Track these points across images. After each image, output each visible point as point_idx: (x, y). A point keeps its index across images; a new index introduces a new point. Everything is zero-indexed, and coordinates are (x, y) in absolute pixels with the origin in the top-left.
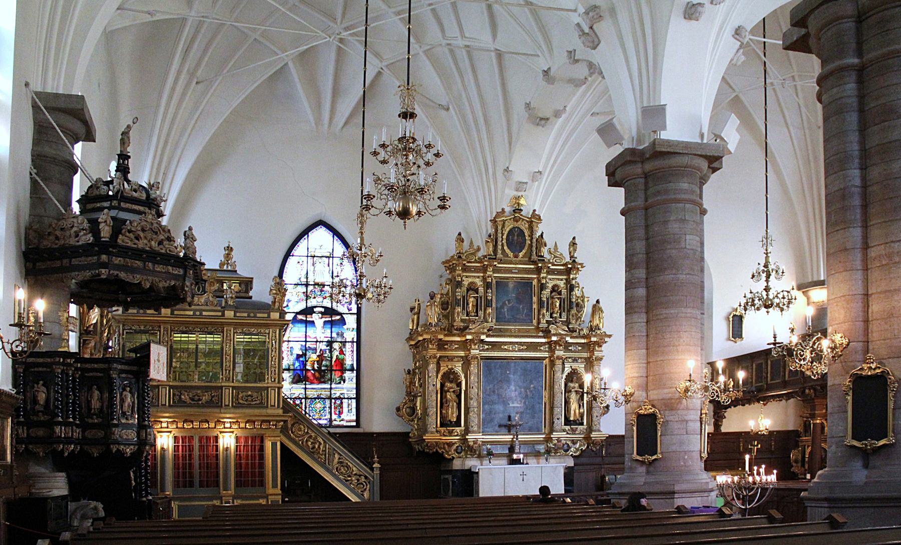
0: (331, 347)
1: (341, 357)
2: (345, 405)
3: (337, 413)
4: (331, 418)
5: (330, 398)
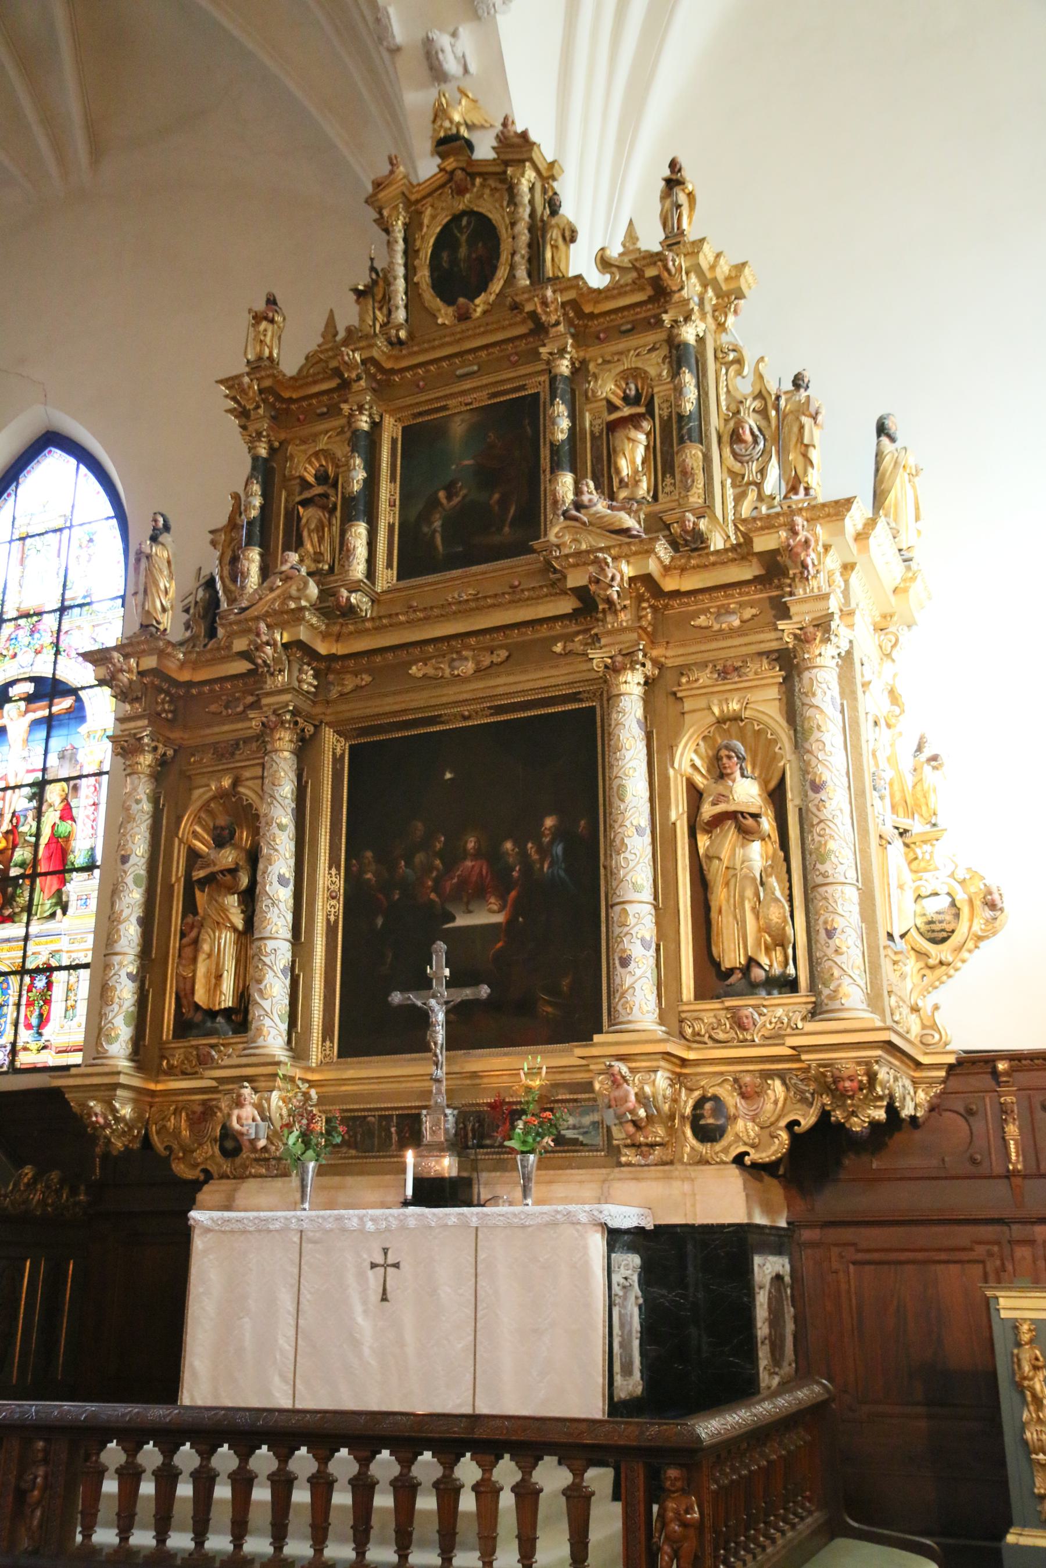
0: (41, 802)
1: (64, 828)
2: (58, 993)
3: (34, 1021)
4: (14, 1044)
5: (22, 971)
